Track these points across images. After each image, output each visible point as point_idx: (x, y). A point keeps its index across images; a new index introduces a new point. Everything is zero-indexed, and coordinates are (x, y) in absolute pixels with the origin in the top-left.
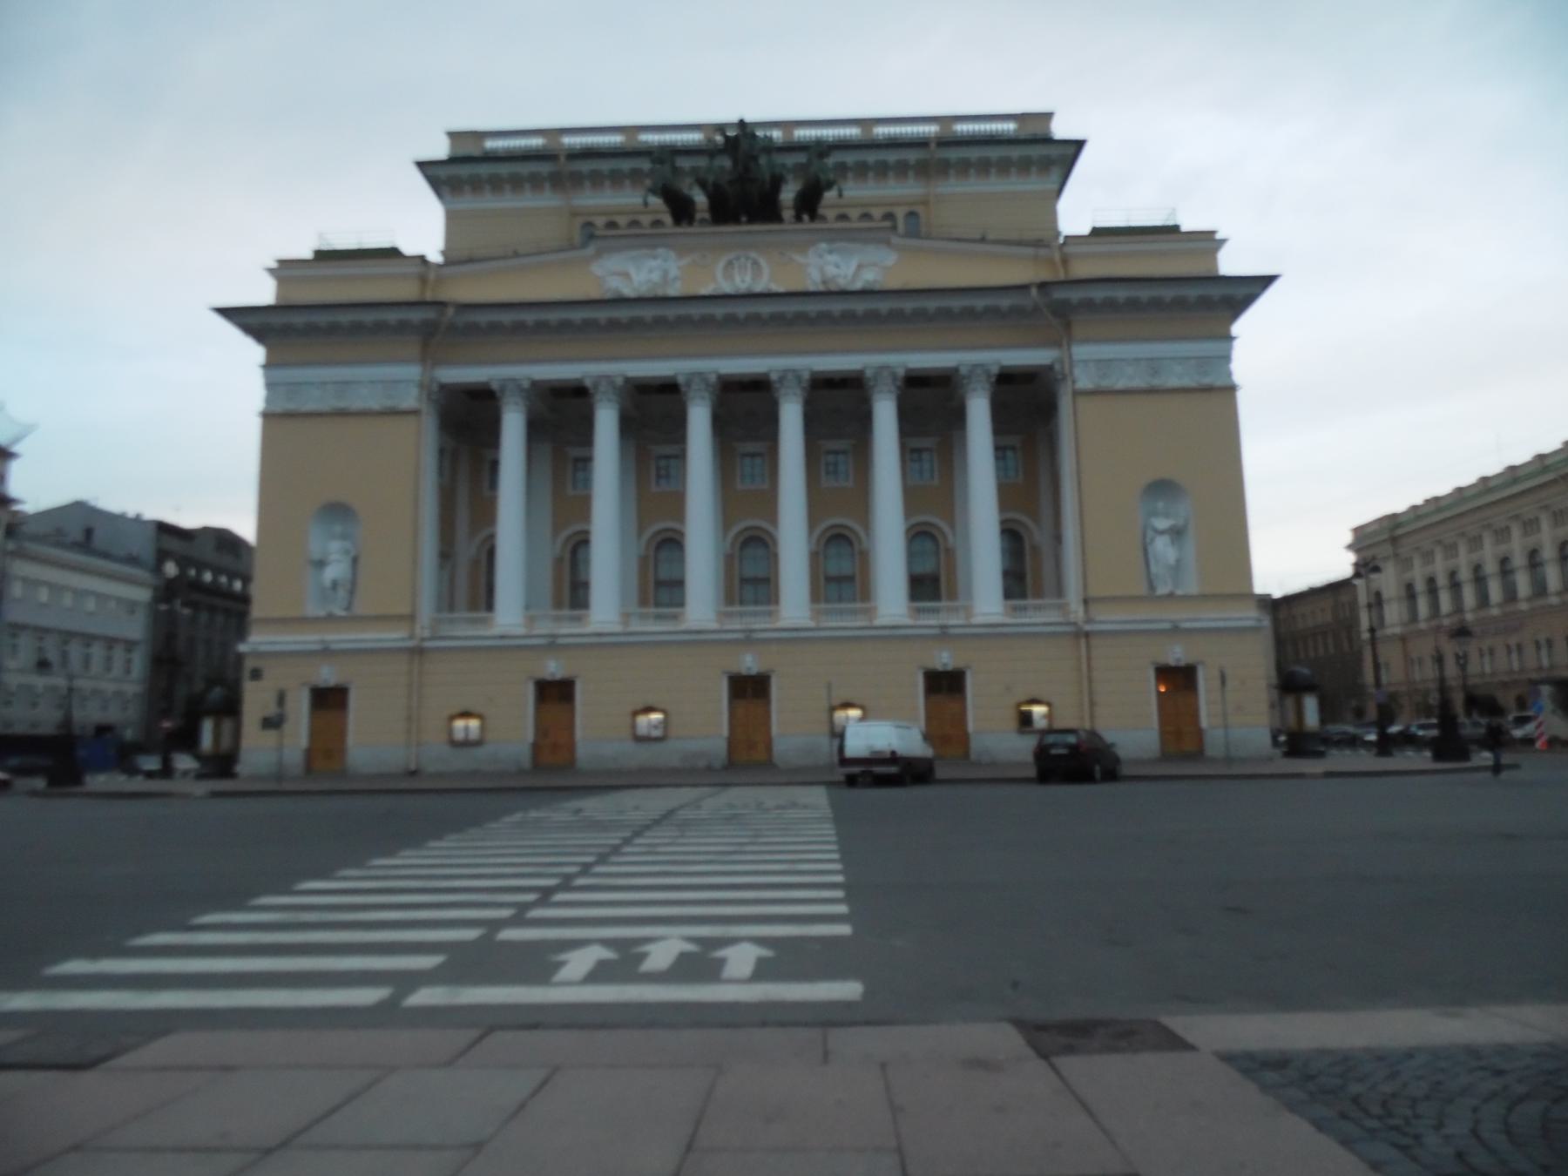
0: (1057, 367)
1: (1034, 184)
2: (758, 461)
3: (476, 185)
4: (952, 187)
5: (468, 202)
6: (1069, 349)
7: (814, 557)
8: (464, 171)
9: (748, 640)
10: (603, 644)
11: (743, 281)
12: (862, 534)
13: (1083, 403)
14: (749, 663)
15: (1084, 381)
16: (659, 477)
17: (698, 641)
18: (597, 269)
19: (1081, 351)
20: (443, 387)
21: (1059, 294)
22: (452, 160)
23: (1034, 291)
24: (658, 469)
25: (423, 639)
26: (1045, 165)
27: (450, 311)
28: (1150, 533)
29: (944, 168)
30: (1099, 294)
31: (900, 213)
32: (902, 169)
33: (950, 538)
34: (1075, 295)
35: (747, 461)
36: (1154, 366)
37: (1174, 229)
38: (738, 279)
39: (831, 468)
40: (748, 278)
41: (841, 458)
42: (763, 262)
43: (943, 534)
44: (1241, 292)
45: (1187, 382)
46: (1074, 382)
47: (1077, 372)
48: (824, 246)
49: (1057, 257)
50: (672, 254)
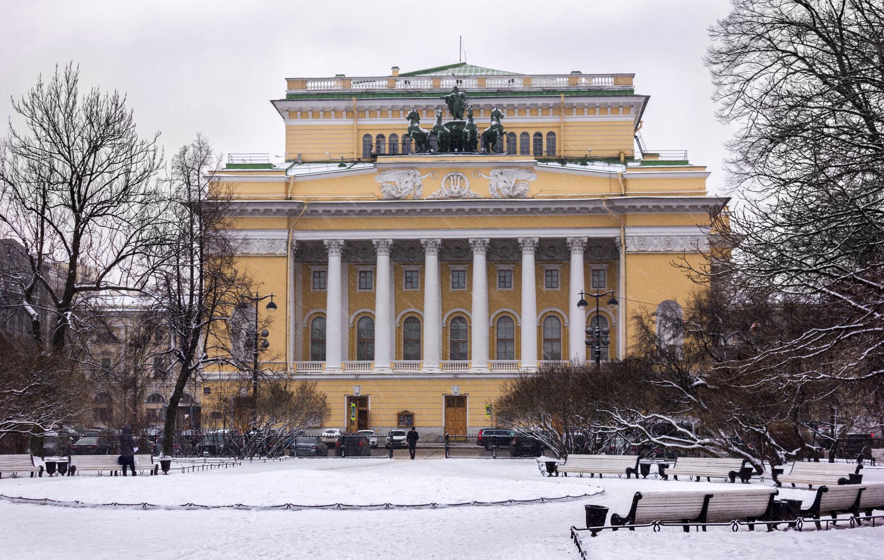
2: (461, 274)
3: (304, 114)
4: (574, 119)
7: (491, 329)
9: (456, 378)
10: (381, 379)
11: (455, 188)
12: (518, 317)
13: (629, 258)
14: (454, 390)
15: (631, 248)
17: (430, 378)
19: (630, 232)
20: (297, 241)
21: (617, 204)
22: (291, 97)
23: (604, 203)
25: (292, 375)
26: (627, 108)
27: (306, 207)
29: (570, 109)
30: (638, 205)
31: (544, 133)
32: (546, 109)
33: (566, 321)
34: (627, 205)
35: (456, 274)
36: (669, 240)
39: (502, 279)
40: (458, 187)
41: (508, 274)
42: (466, 179)
43: (562, 317)
46: (626, 248)
47: (628, 241)
48: (498, 170)
50: (418, 173)
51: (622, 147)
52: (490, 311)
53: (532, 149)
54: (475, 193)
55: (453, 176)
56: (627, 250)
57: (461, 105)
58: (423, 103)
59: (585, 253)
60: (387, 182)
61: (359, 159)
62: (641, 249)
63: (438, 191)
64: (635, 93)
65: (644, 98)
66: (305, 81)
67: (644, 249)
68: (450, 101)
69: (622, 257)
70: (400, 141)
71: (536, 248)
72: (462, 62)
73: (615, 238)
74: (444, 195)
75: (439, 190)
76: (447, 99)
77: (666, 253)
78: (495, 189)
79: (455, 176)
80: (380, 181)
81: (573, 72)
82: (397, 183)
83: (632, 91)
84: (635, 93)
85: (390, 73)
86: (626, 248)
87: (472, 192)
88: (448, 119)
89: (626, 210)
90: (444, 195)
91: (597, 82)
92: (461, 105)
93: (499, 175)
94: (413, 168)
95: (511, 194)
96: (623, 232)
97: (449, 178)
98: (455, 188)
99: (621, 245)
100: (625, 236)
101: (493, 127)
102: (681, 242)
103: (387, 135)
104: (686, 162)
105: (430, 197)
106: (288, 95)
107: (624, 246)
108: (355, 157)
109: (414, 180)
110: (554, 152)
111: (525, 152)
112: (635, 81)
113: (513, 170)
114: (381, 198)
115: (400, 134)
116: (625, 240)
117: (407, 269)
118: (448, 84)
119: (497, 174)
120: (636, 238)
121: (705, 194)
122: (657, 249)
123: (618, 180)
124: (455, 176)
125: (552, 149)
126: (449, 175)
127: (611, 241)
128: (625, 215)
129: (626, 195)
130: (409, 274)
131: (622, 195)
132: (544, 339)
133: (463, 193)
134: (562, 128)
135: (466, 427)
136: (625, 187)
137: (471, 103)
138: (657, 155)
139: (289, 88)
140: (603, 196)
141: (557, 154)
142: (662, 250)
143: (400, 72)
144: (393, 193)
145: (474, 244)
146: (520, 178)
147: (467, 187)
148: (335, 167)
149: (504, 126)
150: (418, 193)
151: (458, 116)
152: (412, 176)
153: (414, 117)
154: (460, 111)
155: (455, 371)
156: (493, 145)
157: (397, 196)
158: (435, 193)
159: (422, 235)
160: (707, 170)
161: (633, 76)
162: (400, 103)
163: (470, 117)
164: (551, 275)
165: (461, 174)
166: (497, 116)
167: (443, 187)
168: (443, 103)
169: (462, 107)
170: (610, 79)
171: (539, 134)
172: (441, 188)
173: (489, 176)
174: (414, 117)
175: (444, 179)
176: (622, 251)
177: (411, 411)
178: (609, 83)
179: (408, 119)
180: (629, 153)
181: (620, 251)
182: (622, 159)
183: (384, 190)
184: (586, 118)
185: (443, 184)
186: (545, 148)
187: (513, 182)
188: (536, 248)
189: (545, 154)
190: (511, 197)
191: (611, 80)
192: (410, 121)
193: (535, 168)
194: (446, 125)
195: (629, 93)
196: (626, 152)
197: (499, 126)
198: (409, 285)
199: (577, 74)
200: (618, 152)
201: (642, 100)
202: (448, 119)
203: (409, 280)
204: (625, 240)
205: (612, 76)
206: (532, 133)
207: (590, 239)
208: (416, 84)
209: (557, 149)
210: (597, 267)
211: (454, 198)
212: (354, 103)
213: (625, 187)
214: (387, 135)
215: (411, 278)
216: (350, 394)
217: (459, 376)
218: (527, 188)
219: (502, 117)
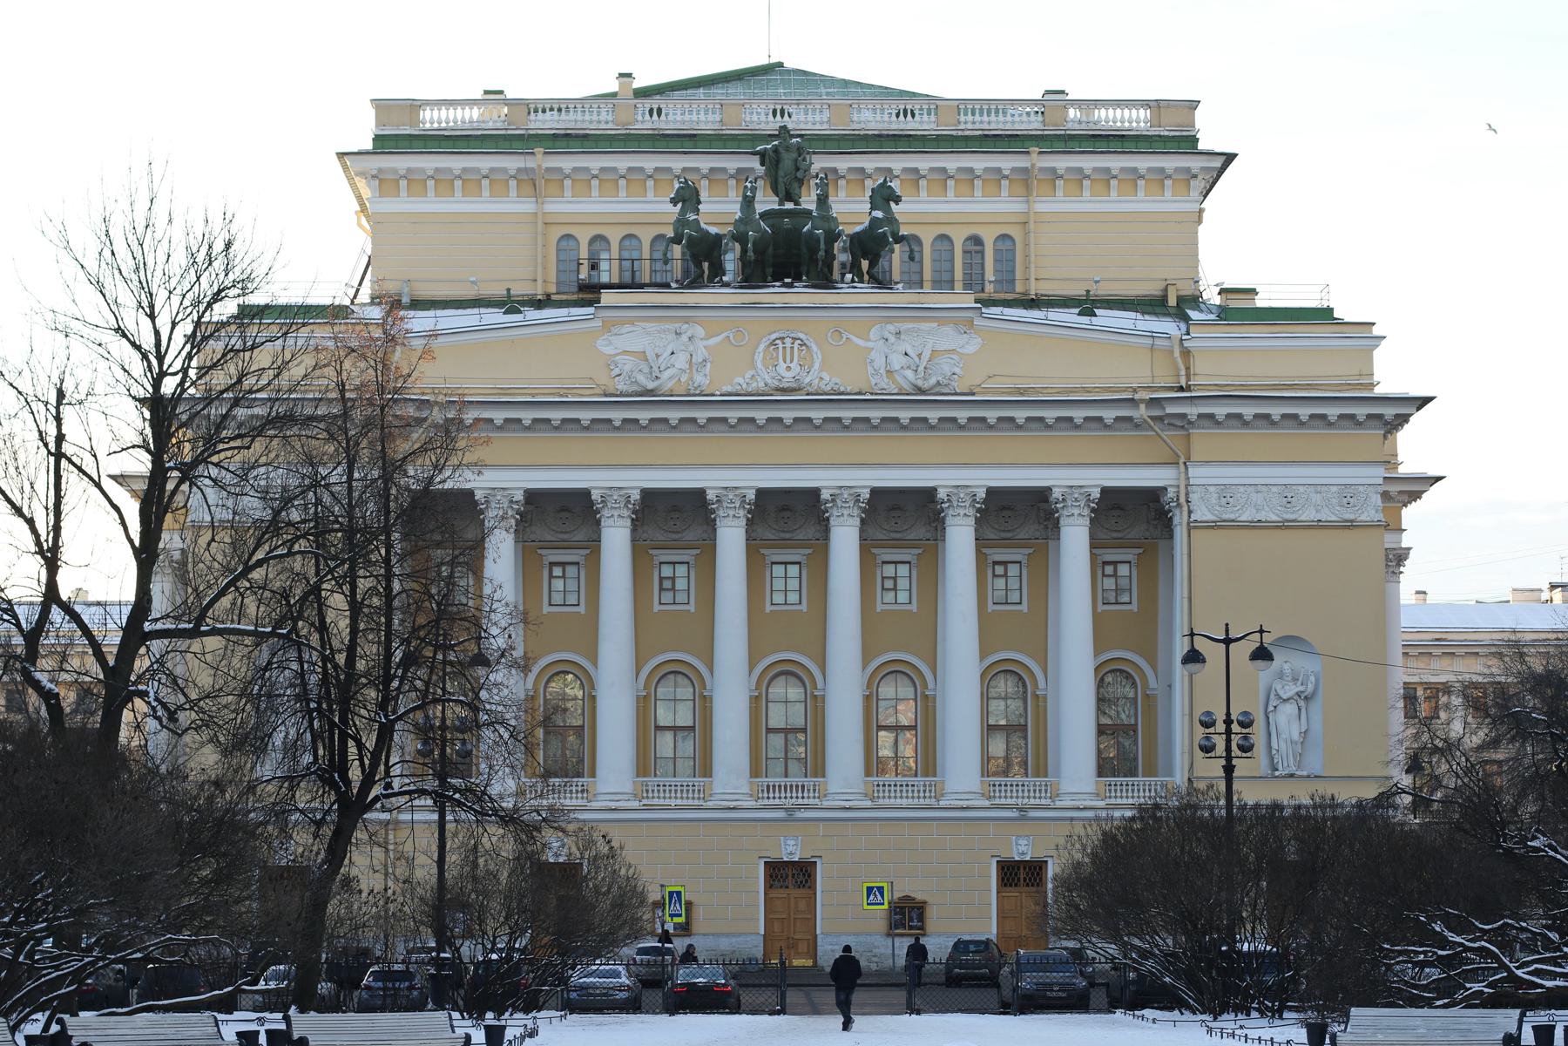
0: (1171, 493)
1: (1169, 203)
3: (416, 183)
5: (404, 204)
6: (1186, 468)
8: (401, 163)
11: (789, 368)
14: (791, 850)
15: (1202, 514)
16: (661, 589)
18: (607, 346)
19: (1198, 474)
21: (1171, 410)
22: (384, 143)
23: (1142, 406)
24: (661, 579)
28: (1273, 702)
33: (1041, 684)
34: (1192, 411)
35: (778, 570)
36: (1288, 494)
37: (1324, 315)
38: (782, 366)
42: (814, 348)
44: (1389, 412)
45: (1327, 515)
46: (1190, 512)
47: (1193, 497)
48: (890, 327)
49: (1177, 353)
50: (700, 331)
51: (1170, 274)
52: (866, 657)
53: (959, 274)
54: (835, 380)
55: (782, 339)
56: (1193, 517)
57: (798, 169)
58: (704, 163)
59: (1095, 523)
60: (625, 352)
61: (548, 296)
62: (1225, 516)
63: (748, 375)
64: (1201, 146)
65: (1224, 158)
66: (414, 106)
67: (1232, 516)
68: (771, 160)
69: (1180, 533)
70: (646, 254)
71: (978, 510)
72: (773, 60)
73: (1165, 489)
74: (761, 385)
75: (752, 372)
76: (763, 156)
77: (1283, 526)
78: (882, 371)
79: (788, 341)
80: (608, 350)
81: (1048, 92)
82: (651, 355)
83: (1194, 140)
84: (1201, 146)
85: (613, 86)
86: (1190, 512)
87: (827, 378)
88: (766, 202)
89: (1190, 423)
90: (761, 385)
91: (1109, 119)
92: (798, 169)
93: (892, 339)
94: (686, 320)
95: (920, 383)
96: (1183, 476)
97: (773, 343)
98: (789, 368)
99: (1179, 505)
100: (1187, 486)
101: (874, 222)
102: (1316, 498)
103: (615, 236)
104: (1329, 311)
105: (729, 389)
106: (379, 139)
107: (1185, 509)
108: (539, 291)
109: (691, 348)
110: (1012, 281)
111: (944, 282)
112: (1199, 113)
113: (925, 326)
114: (612, 391)
115: (646, 236)
116: (1187, 494)
117: (663, 559)
118: (759, 118)
119: (887, 335)
120: (1212, 489)
121: (1372, 386)
122: (1262, 516)
123: (1173, 351)
124: (788, 341)
125: (1007, 277)
126: (774, 336)
127: (1152, 497)
128: (1189, 435)
129: (1188, 389)
130: (667, 571)
131: (1181, 389)
132: (878, 726)
133: (807, 380)
134: (1032, 226)
135: (816, 936)
136: (1188, 369)
137: (819, 163)
138: (1253, 292)
139: (379, 123)
140: (1135, 391)
141: (1019, 288)
142: (1274, 518)
143: (637, 84)
144: (642, 379)
145: (833, 500)
146: (944, 345)
147: (817, 366)
148: (494, 316)
149: (900, 218)
150: (699, 379)
151: (789, 197)
152: (685, 338)
153: (688, 197)
154: (796, 185)
155: (788, 803)
156: (872, 265)
157: (651, 385)
158: (741, 380)
159: (710, 480)
160: (1376, 331)
161: (1193, 105)
162: (649, 163)
163: (823, 201)
164: (1005, 575)
165: (802, 336)
166: (884, 197)
167: (759, 365)
168: (754, 163)
169: (799, 174)
170: (1142, 111)
171: (977, 240)
172: (753, 366)
173: (868, 340)
174: (688, 197)
175: (762, 347)
176: (1180, 520)
177: (919, 896)
178: (1138, 121)
179: (674, 201)
180: (1187, 290)
181: (1176, 521)
182: (1172, 301)
183: (617, 371)
184: (1088, 203)
185: (759, 359)
186: (990, 275)
187: (926, 355)
188: (978, 510)
189: (989, 288)
190: (921, 391)
191: (1143, 114)
192: (680, 205)
193: (978, 322)
194: (764, 215)
195: (1187, 143)
196: (1180, 285)
197: (891, 220)
198: (667, 597)
199: (1055, 99)
200: (1162, 285)
201: (1218, 163)
202: (766, 202)
203: (667, 584)
204: (1187, 494)
205: (1146, 104)
206: (959, 237)
207: (1105, 491)
208: (678, 116)
209: (1019, 275)
210: (1111, 555)
211: (784, 391)
212: (540, 161)
213: (1188, 369)
214: (615, 236)
215: (673, 579)
216: (774, 855)
217: (799, 814)
218: (957, 370)
219: (897, 200)
